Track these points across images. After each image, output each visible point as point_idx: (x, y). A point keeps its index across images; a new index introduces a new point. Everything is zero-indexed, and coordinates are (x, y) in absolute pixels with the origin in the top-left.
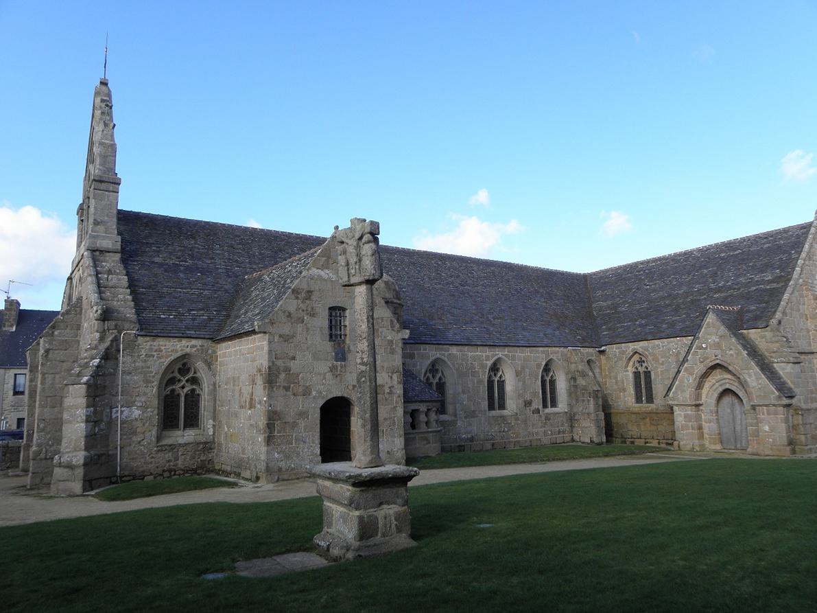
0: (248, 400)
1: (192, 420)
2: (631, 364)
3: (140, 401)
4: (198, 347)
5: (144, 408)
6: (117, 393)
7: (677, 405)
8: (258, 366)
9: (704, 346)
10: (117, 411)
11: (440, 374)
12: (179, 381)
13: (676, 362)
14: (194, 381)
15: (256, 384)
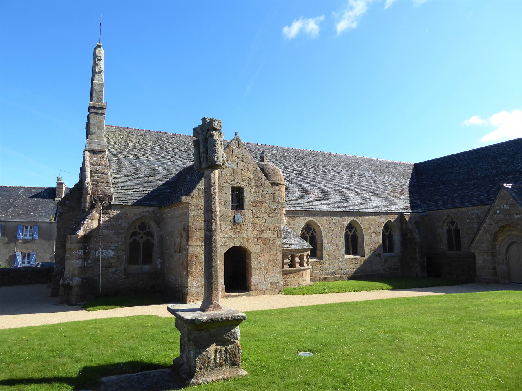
0: (179, 247)
1: (148, 258)
2: (446, 224)
3: (113, 246)
4: (151, 212)
5: (116, 250)
6: (99, 241)
8: (184, 225)
9: (498, 212)
10: (99, 252)
11: (312, 230)
12: (139, 234)
13: (477, 223)
14: (150, 234)
15: (183, 237)
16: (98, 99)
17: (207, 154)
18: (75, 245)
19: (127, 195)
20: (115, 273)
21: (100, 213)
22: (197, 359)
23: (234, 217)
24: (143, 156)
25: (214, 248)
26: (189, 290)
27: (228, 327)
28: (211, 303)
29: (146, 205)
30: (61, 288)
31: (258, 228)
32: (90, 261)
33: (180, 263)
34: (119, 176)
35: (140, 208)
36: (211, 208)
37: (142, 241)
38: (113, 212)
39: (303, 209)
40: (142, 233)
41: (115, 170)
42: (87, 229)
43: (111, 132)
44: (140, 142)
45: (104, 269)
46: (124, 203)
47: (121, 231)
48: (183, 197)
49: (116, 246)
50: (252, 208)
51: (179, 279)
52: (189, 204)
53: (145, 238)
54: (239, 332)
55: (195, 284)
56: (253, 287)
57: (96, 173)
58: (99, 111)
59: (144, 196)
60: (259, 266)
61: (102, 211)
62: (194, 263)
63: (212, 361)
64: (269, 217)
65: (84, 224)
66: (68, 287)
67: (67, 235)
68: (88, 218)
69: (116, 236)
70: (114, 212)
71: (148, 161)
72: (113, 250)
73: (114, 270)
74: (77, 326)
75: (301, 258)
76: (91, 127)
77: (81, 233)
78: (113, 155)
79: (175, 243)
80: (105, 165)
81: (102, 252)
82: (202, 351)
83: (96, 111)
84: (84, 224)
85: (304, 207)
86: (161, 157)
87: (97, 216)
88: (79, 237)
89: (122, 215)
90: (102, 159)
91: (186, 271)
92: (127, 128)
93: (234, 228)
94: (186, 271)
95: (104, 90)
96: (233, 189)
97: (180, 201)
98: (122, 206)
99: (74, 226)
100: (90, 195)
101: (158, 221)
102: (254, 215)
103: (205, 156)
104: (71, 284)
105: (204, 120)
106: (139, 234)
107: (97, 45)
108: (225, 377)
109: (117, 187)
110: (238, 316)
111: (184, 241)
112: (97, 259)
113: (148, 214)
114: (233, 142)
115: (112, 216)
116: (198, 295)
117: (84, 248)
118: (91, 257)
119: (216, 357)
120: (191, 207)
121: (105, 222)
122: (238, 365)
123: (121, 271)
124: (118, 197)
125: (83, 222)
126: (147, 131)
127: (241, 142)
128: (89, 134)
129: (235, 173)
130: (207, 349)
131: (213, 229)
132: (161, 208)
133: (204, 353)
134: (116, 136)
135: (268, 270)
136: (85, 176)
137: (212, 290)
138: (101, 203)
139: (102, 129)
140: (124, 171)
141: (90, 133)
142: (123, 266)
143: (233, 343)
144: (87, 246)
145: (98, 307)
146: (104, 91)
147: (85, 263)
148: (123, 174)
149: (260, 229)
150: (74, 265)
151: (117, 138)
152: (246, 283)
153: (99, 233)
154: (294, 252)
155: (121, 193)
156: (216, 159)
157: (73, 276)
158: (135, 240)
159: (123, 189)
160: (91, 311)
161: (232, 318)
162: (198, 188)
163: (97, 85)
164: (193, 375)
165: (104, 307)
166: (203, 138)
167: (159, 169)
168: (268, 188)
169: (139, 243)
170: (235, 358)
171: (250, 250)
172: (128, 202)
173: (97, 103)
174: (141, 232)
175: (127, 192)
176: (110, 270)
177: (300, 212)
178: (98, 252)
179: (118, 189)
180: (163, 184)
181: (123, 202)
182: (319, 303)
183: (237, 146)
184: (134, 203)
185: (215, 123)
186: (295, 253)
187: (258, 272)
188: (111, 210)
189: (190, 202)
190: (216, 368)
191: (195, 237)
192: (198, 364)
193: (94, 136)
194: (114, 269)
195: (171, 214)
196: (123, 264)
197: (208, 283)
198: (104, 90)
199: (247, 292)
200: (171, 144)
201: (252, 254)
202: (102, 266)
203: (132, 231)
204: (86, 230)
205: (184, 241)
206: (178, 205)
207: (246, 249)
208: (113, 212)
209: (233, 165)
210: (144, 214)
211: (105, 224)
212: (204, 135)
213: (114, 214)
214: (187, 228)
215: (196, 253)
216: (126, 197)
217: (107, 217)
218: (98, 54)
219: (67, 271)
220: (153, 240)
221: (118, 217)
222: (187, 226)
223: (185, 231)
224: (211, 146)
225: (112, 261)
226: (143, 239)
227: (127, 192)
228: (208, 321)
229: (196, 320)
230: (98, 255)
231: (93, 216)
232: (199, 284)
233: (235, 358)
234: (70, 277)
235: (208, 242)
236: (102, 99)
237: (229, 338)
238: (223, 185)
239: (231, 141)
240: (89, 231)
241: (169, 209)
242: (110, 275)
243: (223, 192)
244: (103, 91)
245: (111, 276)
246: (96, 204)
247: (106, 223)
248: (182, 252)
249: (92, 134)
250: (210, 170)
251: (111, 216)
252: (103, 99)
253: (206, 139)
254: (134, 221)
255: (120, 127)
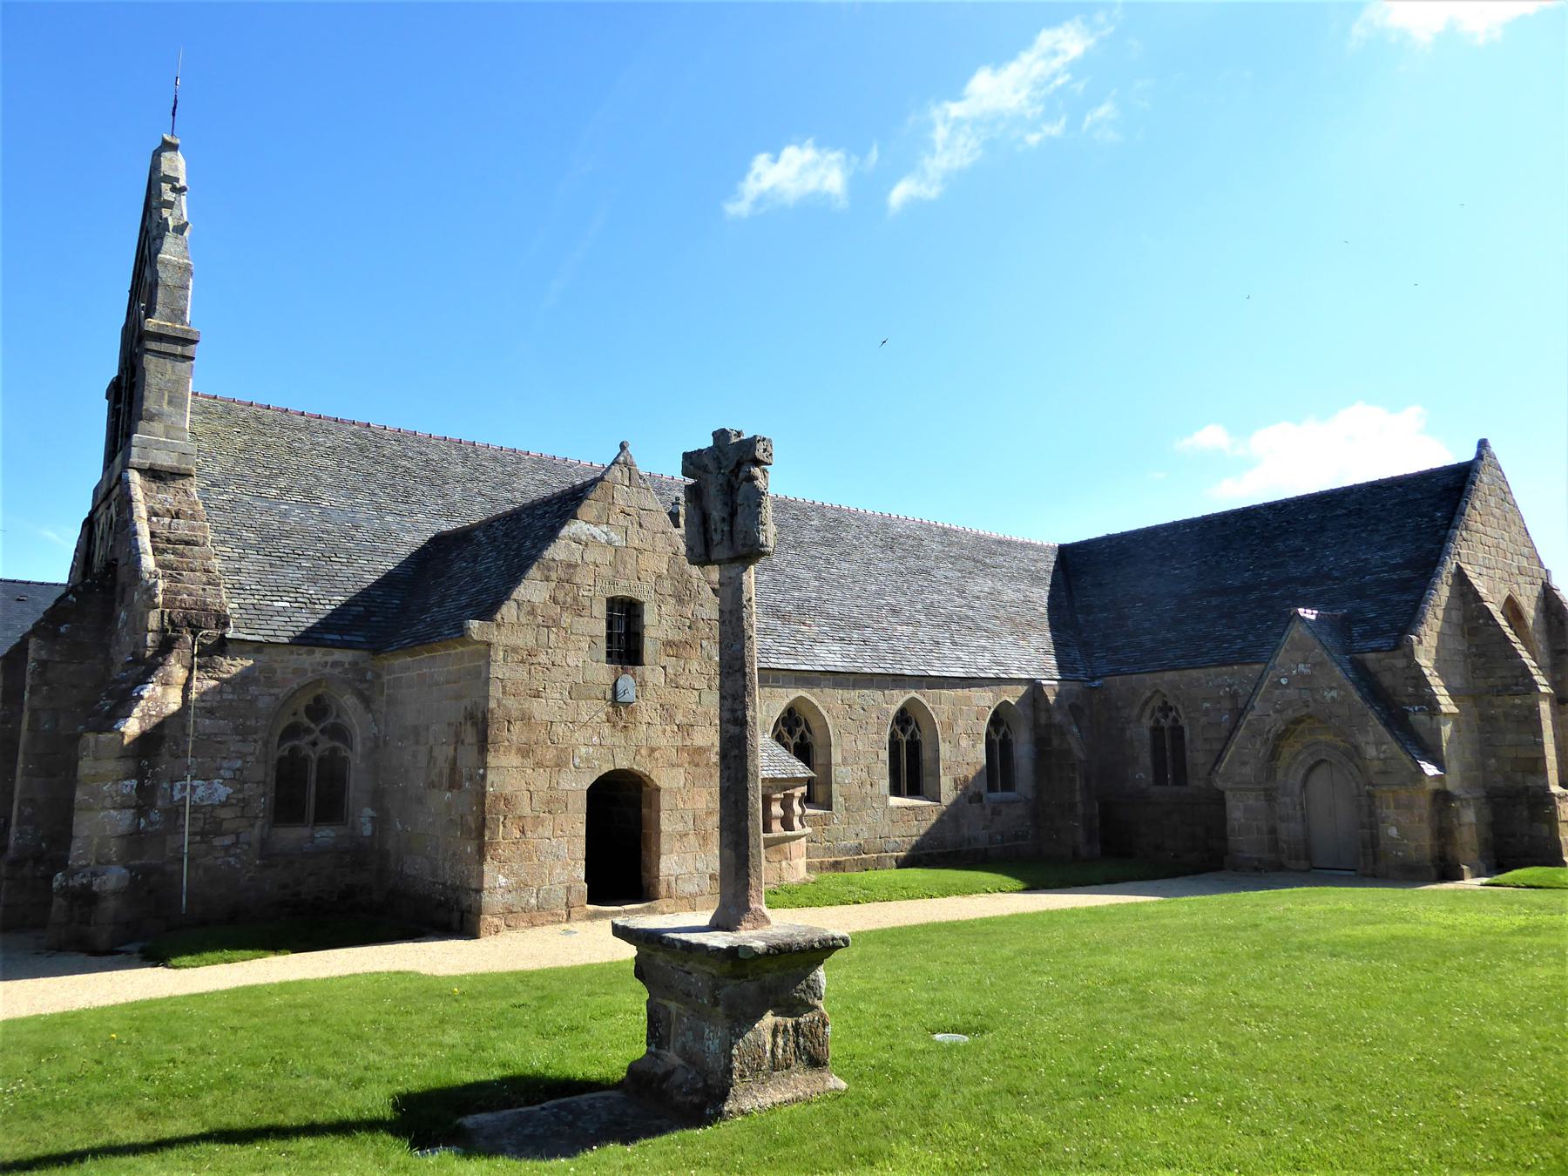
0: (446, 771)
1: (332, 808)
2: (1148, 712)
3: (228, 769)
4: (347, 666)
5: (238, 779)
6: (185, 752)
7: (1231, 790)
8: (469, 708)
9: (1284, 681)
10: (184, 788)
11: (803, 727)
12: (308, 731)
13: (1231, 710)
14: (339, 733)
15: (462, 742)
16: (172, 310)
17: (731, 525)
18: (110, 766)
19: (271, 613)
20: (232, 852)
21: (189, 665)
22: (735, 1052)
23: (615, 685)
24: (307, 492)
25: (751, 768)
26: (486, 898)
27: (800, 969)
28: (746, 908)
29: (334, 645)
30: (59, 902)
31: (679, 718)
32: (155, 816)
33: (451, 820)
34: (239, 553)
35: (314, 652)
36: (743, 665)
37: (315, 754)
38: (230, 662)
39: (779, 667)
40: (317, 730)
41: (227, 533)
42: (151, 716)
43: (200, 414)
44: (293, 451)
45: (198, 838)
46: (266, 638)
47: (253, 722)
48: (474, 624)
49: (238, 769)
50: (665, 660)
51: (444, 869)
52: (489, 644)
53: (325, 744)
54: (825, 981)
55: (502, 880)
56: (663, 889)
57: (169, 541)
58: (174, 347)
59: (322, 616)
60: (680, 827)
61: (196, 659)
62: (502, 819)
63: (768, 1055)
64: (710, 687)
65: (141, 698)
66: (86, 898)
67: (81, 735)
68: (154, 679)
69: (240, 738)
70: (234, 662)
71: (323, 511)
72: (226, 782)
73: (230, 843)
74: (142, 1015)
75: (786, 804)
76: (149, 397)
77: (132, 727)
78: (214, 485)
79: (431, 758)
80: (193, 517)
81: (191, 786)
82: (745, 1030)
83: (164, 347)
84: (141, 698)
85: (781, 661)
86: (360, 498)
87: (178, 672)
88: (126, 741)
89: (257, 674)
90: (181, 496)
91: (477, 842)
92: (251, 404)
93: (614, 718)
94: (477, 842)
95: (191, 284)
96: (613, 603)
97: (461, 632)
98: (258, 647)
99: (106, 705)
100: (159, 610)
101: (367, 693)
102: (668, 680)
103: (725, 529)
104: (94, 888)
105: (721, 436)
106: (308, 731)
107: (165, 142)
108: (801, 1094)
109: (236, 586)
110: (833, 939)
111: (468, 757)
112: (174, 812)
113: (336, 671)
114: (616, 470)
115: (229, 676)
116: (512, 912)
117: (140, 774)
118: (159, 803)
119: (775, 1044)
120: (496, 654)
121: (204, 693)
122: (825, 1064)
123: (249, 845)
124: (244, 616)
125: (138, 693)
126: (312, 416)
127: (637, 471)
128: (141, 419)
129: (619, 559)
130: (757, 1025)
131: (749, 719)
132: (379, 654)
133: (749, 1035)
134: (217, 425)
135: (705, 839)
136: (138, 549)
137: (748, 875)
138: (195, 635)
139: (182, 405)
140: (251, 537)
141: (144, 413)
142: (256, 831)
143: (813, 1008)
144: (149, 766)
145: (208, 955)
146: (191, 288)
147: (142, 820)
148: (251, 547)
149: (685, 721)
150: (108, 828)
151: (222, 435)
152: (640, 877)
153: (184, 727)
154: (770, 787)
155: (251, 607)
156: (762, 538)
157: (102, 861)
158: (293, 750)
159: (256, 592)
160: (185, 967)
161: (820, 943)
162: (515, 600)
163: (170, 267)
164: (727, 1093)
165: (227, 954)
166: (721, 481)
167: (359, 535)
168: (707, 605)
169: (306, 759)
170: (817, 1045)
171: (656, 780)
172: (278, 633)
173: (169, 324)
174: (313, 726)
175: (269, 603)
176: (217, 842)
177: (771, 672)
178: (179, 787)
179: (241, 592)
180: (377, 582)
181: (262, 632)
182: (886, 924)
183: (627, 483)
184: (296, 637)
185: (760, 446)
186: (770, 791)
187: (678, 844)
188: (225, 658)
189: (494, 640)
190: (776, 1073)
191: (506, 743)
192: (736, 1064)
193: (157, 426)
194: (228, 840)
195: (416, 673)
196: (259, 823)
197: (738, 857)
198: (191, 283)
199: (647, 904)
200: (388, 461)
201: (662, 793)
202: (192, 829)
203: (284, 724)
204: (147, 717)
205: (468, 757)
206: (446, 648)
207: (645, 778)
208: (230, 662)
209: (612, 534)
210: (328, 670)
211: (203, 701)
212: (723, 474)
213: (234, 670)
214: (480, 715)
215: (508, 790)
216: (268, 618)
217: (211, 678)
218: (166, 168)
219: (79, 848)
220: (348, 750)
221: (245, 678)
222: (481, 709)
223: (475, 724)
224: (749, 506)
225: (224, 814)
226: (320, 747)
227: (269, 603)
228: (768, 950)
229: (740, 950)
230: (179, 797)
231: (169, 675)
232: (513, 880)
233: (817, 1045)
234: (88, 865)
235: (735, 752)
236: (184, 313)
237: (803, 995)
238: (586, 593)
239: (609, 468)
240: (155, 720)
241: (409, 659)
242: (217, 858)
243: (586, 612)
244: (187, 288)
245: (219, 862)
246: (177, 639)
247: (208, 698)
248: (460, 786)
249: (151, 418)
250: (737, 566)
251: (225, 676)
252: (188, 312)
253: (728, 485)
254: (294, 693)
255: (228, 400)
